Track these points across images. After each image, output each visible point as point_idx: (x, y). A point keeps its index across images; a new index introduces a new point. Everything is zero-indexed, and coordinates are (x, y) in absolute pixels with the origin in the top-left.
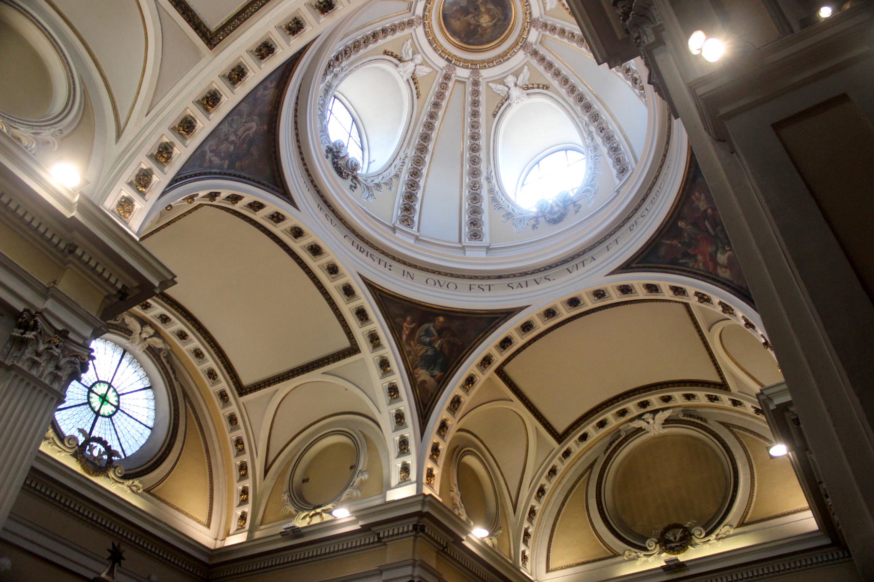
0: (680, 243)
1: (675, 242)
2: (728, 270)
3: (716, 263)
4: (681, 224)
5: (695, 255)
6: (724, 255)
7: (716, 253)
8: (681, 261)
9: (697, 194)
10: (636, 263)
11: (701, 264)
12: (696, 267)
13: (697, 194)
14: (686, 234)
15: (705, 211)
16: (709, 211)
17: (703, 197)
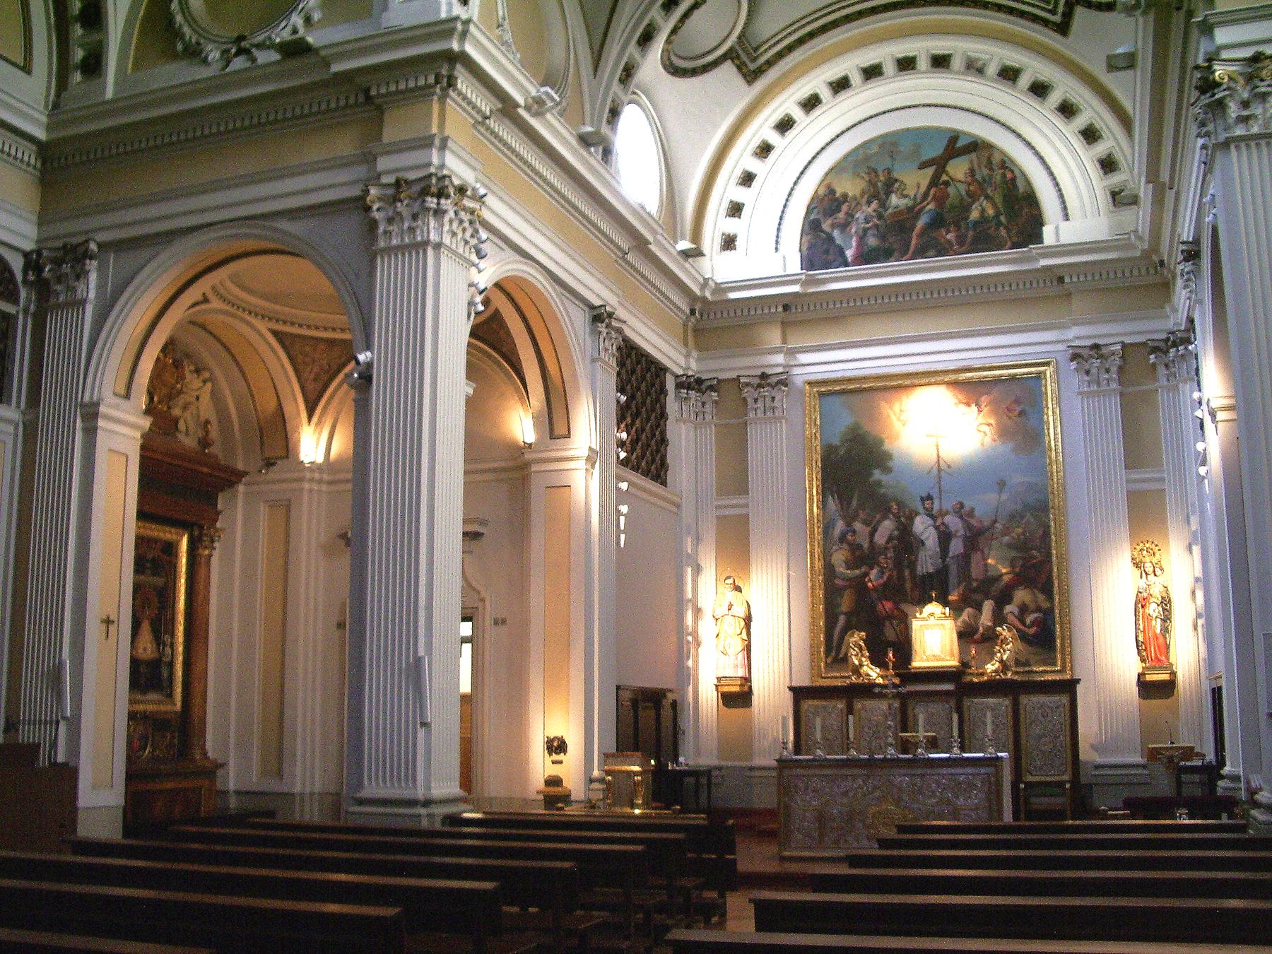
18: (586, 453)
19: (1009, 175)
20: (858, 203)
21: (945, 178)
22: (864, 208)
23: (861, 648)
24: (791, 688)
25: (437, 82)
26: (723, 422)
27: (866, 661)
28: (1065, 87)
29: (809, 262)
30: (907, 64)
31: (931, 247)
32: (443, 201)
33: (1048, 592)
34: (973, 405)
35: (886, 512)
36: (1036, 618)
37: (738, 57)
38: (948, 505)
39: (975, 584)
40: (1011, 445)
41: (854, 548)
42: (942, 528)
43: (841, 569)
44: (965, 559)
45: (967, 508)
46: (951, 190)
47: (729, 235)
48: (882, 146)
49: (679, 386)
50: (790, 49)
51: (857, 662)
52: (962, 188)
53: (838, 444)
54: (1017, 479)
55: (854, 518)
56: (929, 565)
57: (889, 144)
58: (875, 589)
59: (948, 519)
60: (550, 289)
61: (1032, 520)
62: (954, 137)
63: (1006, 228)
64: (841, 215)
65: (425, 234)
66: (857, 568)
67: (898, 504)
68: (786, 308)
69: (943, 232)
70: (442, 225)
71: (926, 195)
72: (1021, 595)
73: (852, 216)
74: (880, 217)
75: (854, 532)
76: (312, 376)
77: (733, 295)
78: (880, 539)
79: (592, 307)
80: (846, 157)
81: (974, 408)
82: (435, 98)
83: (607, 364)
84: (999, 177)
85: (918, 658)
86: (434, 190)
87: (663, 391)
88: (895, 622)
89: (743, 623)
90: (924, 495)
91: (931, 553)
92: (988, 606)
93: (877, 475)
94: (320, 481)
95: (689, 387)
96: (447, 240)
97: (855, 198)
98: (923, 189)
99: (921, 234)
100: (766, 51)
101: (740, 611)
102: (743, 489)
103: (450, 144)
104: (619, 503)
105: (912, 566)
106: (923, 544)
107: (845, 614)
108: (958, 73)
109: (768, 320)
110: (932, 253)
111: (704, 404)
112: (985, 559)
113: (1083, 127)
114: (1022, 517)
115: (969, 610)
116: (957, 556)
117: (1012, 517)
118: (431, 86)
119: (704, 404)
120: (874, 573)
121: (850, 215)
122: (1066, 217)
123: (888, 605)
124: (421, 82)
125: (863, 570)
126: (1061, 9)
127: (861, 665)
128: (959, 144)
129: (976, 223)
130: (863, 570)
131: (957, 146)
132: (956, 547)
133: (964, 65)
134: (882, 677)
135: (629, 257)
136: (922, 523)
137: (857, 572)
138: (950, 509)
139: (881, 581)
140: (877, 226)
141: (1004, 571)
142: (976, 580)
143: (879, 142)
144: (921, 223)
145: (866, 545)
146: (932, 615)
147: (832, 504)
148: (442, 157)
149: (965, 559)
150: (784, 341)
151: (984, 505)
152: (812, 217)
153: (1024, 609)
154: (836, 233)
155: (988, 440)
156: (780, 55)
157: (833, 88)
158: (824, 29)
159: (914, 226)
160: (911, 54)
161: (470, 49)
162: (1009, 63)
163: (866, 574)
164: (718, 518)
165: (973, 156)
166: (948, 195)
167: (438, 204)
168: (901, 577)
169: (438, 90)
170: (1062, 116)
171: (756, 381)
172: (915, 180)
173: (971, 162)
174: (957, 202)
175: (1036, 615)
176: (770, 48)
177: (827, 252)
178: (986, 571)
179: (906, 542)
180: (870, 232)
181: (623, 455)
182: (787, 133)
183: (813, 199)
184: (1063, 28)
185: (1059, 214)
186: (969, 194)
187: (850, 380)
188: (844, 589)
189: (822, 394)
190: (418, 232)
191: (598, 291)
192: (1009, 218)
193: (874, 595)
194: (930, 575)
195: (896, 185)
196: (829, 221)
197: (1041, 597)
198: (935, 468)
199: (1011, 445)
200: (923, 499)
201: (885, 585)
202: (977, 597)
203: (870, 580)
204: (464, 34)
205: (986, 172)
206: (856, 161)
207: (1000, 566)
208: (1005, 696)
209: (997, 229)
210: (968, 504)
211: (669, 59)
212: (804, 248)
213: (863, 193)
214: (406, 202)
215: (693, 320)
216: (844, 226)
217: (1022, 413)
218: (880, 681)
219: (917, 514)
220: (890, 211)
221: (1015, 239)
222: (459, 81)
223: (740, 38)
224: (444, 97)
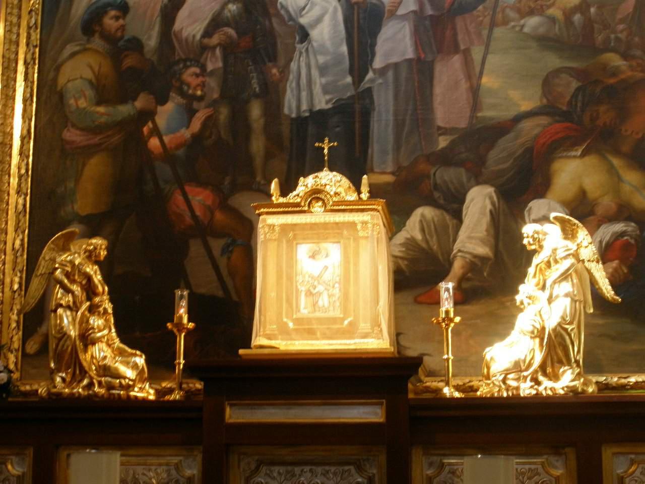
23: (90, 290)
39: (443, 142)
56: (317, 89)
58: (168, 155)
66: (123, 101)
85: (272, 327)
88: (217, 245)
91: (321, 59)
106: (304, 35)
115: (424, 212)
116: (396, 66)
120: (166, 114)
123: (200, 198)
125: (140, 103)
130: (140, 103)
137: (125, 110)
139: (186, 134)
141: (526, 106)
142: (444, 131)
145: (152, 41)
163: (147, 115)
175: (619, 227)
178: (476, 105)
188: (88, 151)
193: (164, 170)
194: (319, 118)
201: (197, 138)
202: (446, 175)
203: (156, 132)
207: (515, 94)
208: (556, 449)
218: (146, 392)
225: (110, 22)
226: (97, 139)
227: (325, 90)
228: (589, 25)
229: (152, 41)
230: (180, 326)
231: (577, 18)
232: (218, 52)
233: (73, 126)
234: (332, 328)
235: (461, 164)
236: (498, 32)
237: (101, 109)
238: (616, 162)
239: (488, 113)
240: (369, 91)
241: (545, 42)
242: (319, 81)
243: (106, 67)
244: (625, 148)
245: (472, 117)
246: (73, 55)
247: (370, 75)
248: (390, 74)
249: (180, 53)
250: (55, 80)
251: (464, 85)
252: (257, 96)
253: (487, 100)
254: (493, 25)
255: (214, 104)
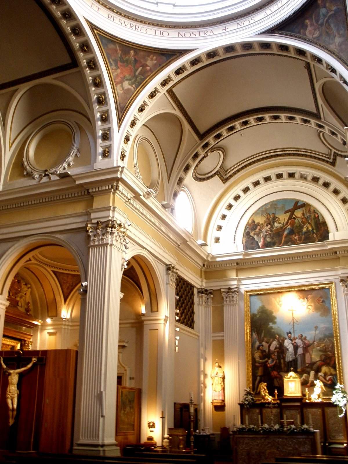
0: (121, 55)
1: (120, 52)
2: (122, 91)
3: (121, 82)
4: (132, 52)
5: (118, 68)
6: (129, 85)
7: (127, 80)
8: (111, 60)
9: (155, 58)
10: (97, 33)
11: (116, 73)
12: (113, 71)
13: (155, 58)
14: (127, 57)
15: (147, 66)
16: (148, 68)
17: (155, 62)
18: (164, 318)
19: (317, 215)
20: (263, 226)
21: (294, 216)
22: (265, 227)
23: (265, 390)
24: (239, 404)
25: (112, 188)
26: (214, 305)
27: (267, 394)
28: (335, 184)
29: (246, 247)
30: (279, 176)
31: (290, 241)
32: (113, 229)
33: (334, 367)
34: (305, 299)
35: (274, 338)
36: (330, 378)
37: (220, 174)
38: (297, 336)
39: (307, 365)
40: (319, 313)
41: (263, 351)
42: (295, 344)
43: (258, 359)
44: (303, 355)
45: (304, 337)
46: (296, 221)
47: (217, 238)
48: (271, 205)
49: (199, 292)
50: (238, 171)
51: (263, 395)
52: (300, 220)
53: (257, 313)
54: (322, 326)
55: (263, 341)
56: (290, 358)
57: (274, 205)
58: (271, 367)
59: (297, 341)
60: (151, 258)
61: (328, 341)
62: (297, 202)
63: (316, 234)
64: (257, 230)
65: (107, 241)
67: (279, 335)
68: (237, 264)
69: (294, 236)
70: (113, 238)
71: (287, 222)
72: (324, 369)
73: (261, 230)
74: (271, 231)
75: (263, 346)
76: (67, 287)
77: (218, 259)
78: (272, 348)
79: (167, 265)
80: (259, 209)
81: (306, 300)
82: (112, 193)
83: (171, 285)
84: (313, 216)
85: (286, 393)
86: (110, 225)
87: (193, 294)
88: (278, 379)
89: (222, 380)
90: (288, 332)
91: (291, 353)
92: (312, 373)
93: (271, 325)
94: (68, 325)
95: (202, 293)
96: (114, 243)
97: (262, 224)
98: (286, 221)
99: (285, 237)
100: (230, 172)
101: (221, 375)
102: (223, 331)
103: (116, 209)
104: (176, 335)
105: (284, 358)
106: (288, 350)
107: (260, 376)
108: (298, 179)
109: (231, 269)
110: (290, 243)
111: (208, 299)
112: (311, 355)
113: (342, 198)
114: (324, 340)
115: (305, 375)
116: (300, 354)
117: (320, 339)
118: (109, 189)
119: (208, 299)
120: (270, 361)
121: (260, 230)
122: (337, 230)
123: (275, 373)
124: (107, 188)
126: (332, 157)
127: (265, 395)
128: (299, 204)
129: (305, 232)
130: (266, 359)
131: (298, 205)
132: (300, 351)
133: (300, 176)
134: (273, 400)
135: (180, 247)
136: (288, 342)
137: (264, 361)
138: (298, 337)
139: (273, 364)
140: (269, 234)
141: (318, 360)
142: (308, 363)
143: (271, 204)
144: (286, 233)
145: (267, 351)
146: (291, 376)
147: (255, 335)
148: (113, 214)
149: (303, 355)
150: (237, 276)
151: (310, 335)
152: (247, 231)
153: (325, 374)
154: (255, 237)
155: (311, 312)
156: (235, 173)
157: (254, 185)
158: (250, 164)
159: (282, 235)
160: (281, 173)
161: (124, 177)
162: (315, 176)
163: (267, 361)
164: (213, 341)
165: (304, 208)
166: (295, 222)
167: (112, 230)
168: (280, 363)
169: (113, 191)
170: (334, 194)
171: (227, 290)
172: (283, 218)
173: (303, 211)
174: (298, 225)
175: (330, 377)
176: (231, 171)
177: (252, 243)
178: (311, 360)
179: (282, 349)
180: (268, 236)
181: (177, 318)
182: (237, 201)
183: (247, 224)
184: (333, 164)
185: (335, 229)
186: (302, 222)
187: (261, 290)
189: (250, 295)
190: (105, 240)
191: (169, 259)
192: (317, 231)
193: (270, 369)
194: (291, 361)
195: (277, 219)
196: (253, 232)
197: (332, 370)
198: (292, 323)
199: (319, 313)
200: (288, 334)
201: (274, 365)
202: (308, 370)
203: (268, 364)
204: (122, 172)
205: (308, 214)
206: (263, 210)
207: (316, 358)
209: (313, 235)
210: (304, 335)
211: (195, 175)
212: (244, 242)
213: (265, 222)
214: (101, 229)
215: (204, 268)
216: (258, 234)
217: (323, 301)
219: (286, 339)
220: (275, 228)
221: (319, 238)
222: (120, 188)
223: (220, 167)
224: (114, 194)
225: (261, 348)
226: (260, 365)
227: (292, 358)
228: (326, 348)
229: (267, 351)
230: (276, 394)
231: (324, 347)
232: (276, 352)
233: (257, 363)
234: (293, 393)
235: (309, 368)
236: (314, 349)
237: (261, 360)
238: (330, 367)
239: (313, 361)
240: (297, 358)
241: (320, 351)
242: (290, 356)
243: (261, 355)
244: (331, 365)
245: (311, 362)
246: (256, 352)
247: (297, 356)
248: (300, 355)
249: (271, 353)
250: (254, 356)
251: (309, 357)
252: (282, 359)
253: (313, 359)
254: (313, 348)
255: (276, 360)
